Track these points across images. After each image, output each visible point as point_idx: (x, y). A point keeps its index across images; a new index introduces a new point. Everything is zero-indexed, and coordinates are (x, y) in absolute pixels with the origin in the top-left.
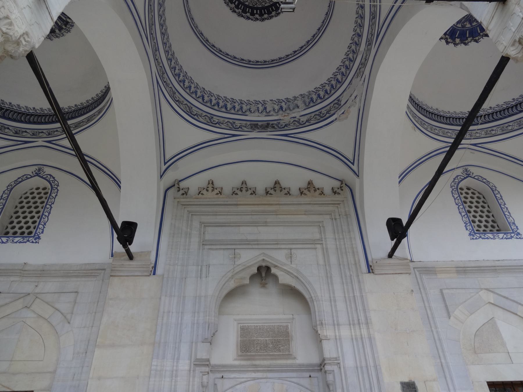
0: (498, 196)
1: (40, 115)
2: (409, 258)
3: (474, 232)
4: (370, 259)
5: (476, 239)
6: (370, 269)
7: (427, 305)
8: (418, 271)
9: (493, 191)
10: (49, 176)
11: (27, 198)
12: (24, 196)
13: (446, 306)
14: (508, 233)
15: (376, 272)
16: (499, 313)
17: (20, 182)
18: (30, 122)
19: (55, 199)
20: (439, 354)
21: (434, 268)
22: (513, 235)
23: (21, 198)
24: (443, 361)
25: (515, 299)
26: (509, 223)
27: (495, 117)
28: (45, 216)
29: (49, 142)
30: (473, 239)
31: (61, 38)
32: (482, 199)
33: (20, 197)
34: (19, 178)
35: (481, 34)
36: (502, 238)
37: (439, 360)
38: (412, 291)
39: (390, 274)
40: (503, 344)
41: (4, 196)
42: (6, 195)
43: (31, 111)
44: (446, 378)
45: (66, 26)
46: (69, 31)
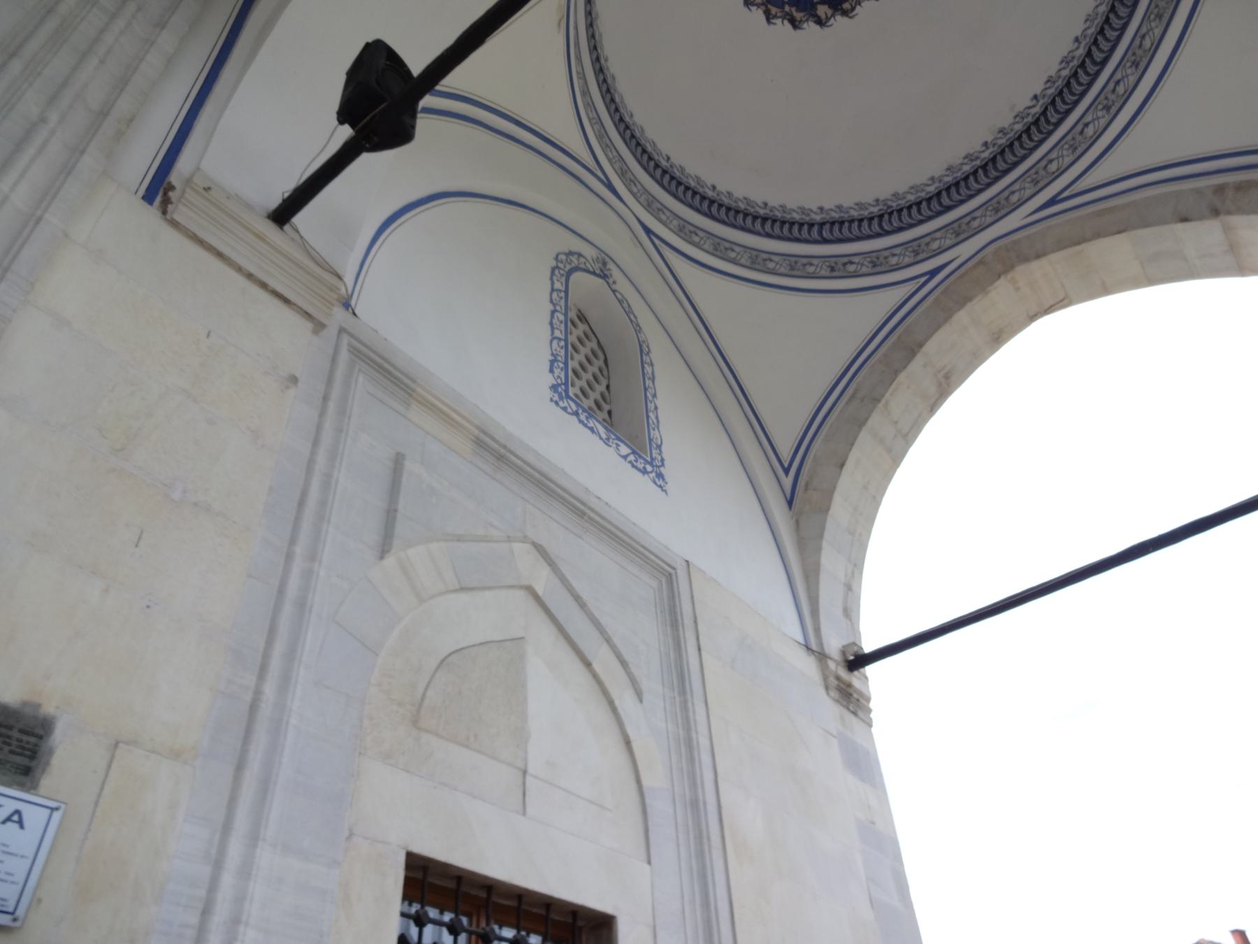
0: (648, 369)
2: (349, 279)
3: (566, 391)
4: (184, 164)
5: (565, 409)
6: (158, 189)
7: (321, 459)
8: (353, 351)
9: (641, 351)
13: (391, 516)
14: (641, 457)
15: (180, 213)
16: (542, 636)
20: (266, 656)
21: (414, 381)
22: (649, 468)
24: (269, 690)
25: (604, 620)
26: (650, 440)
27: (714, 209)
30: (557, 403)
32: (601, 363)
35: (787, 8)
36: (625, 457)
37: (250, 680)
38: (294, 380)
39: (239, 269)
40: (521, 736)
44: (240, 767)
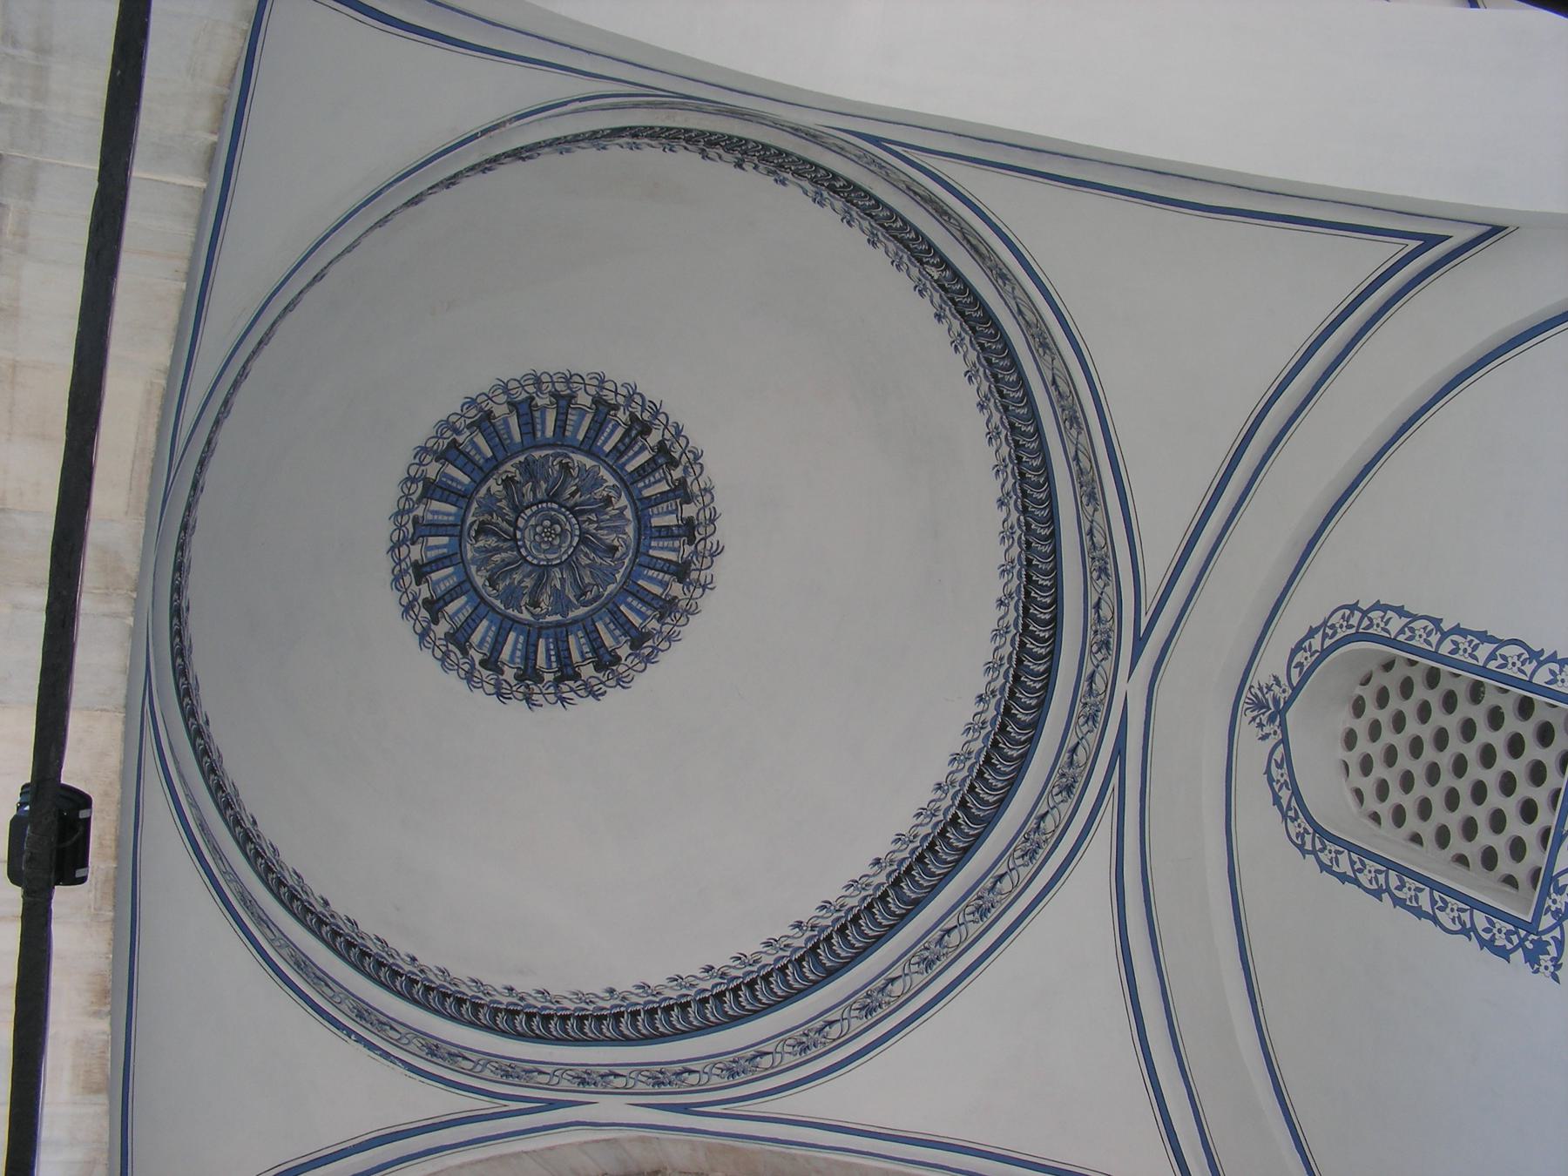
1: (1016, 678)
10: (1299, 658)
11: (1382, 790)
12: (1372, 803)
17: (1296, 793)
18: (1037, 726)
19: (1415, 618)
23: (1375, 817)
28: (1492, 657)
29: (1140, 642)
31: (719, 504)
33: (1371, 824)
34: (1277, 800)
41: (1344, 866)
42: (1344, 858)
43: (991, 713)
45: (674, 463)
46: (697, 457)
